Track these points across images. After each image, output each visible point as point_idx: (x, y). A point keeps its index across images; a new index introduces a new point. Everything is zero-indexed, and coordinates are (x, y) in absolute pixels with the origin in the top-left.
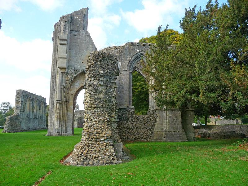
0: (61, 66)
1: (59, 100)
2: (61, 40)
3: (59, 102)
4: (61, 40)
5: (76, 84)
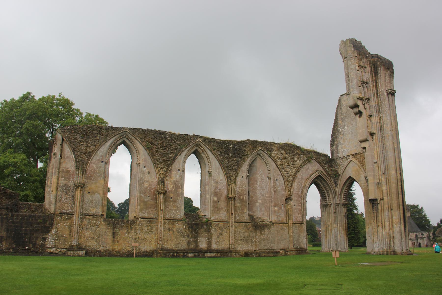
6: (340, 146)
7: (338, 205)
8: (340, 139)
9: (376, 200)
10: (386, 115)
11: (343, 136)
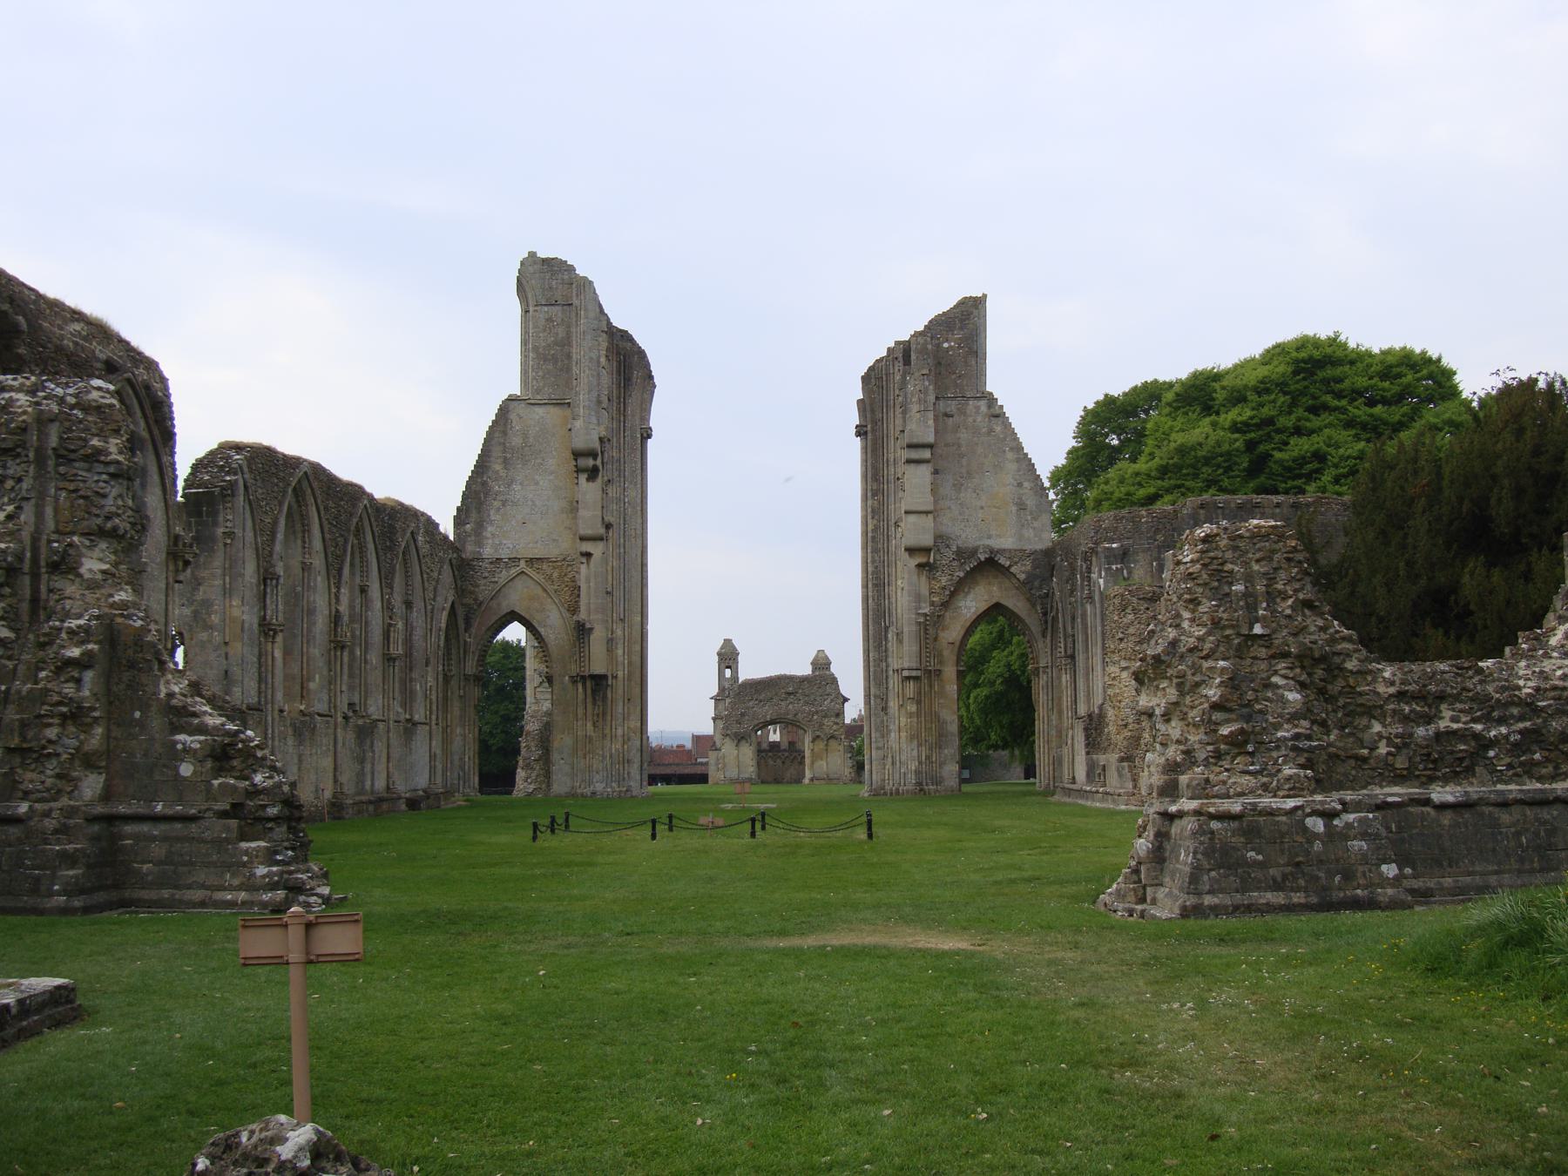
0: (912, 540)
1: (914, 665)
2: (910, 446)
3: (914, 673)
4: (910, 446)
5: (962, 604)
6: (489, 529)
7: (467, 678)
8: (492, 512)
9: (604, 677)
10: (636, 485)
11: (503, 505)
